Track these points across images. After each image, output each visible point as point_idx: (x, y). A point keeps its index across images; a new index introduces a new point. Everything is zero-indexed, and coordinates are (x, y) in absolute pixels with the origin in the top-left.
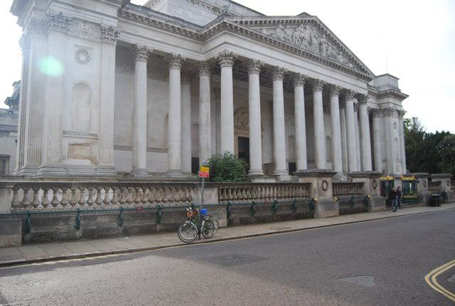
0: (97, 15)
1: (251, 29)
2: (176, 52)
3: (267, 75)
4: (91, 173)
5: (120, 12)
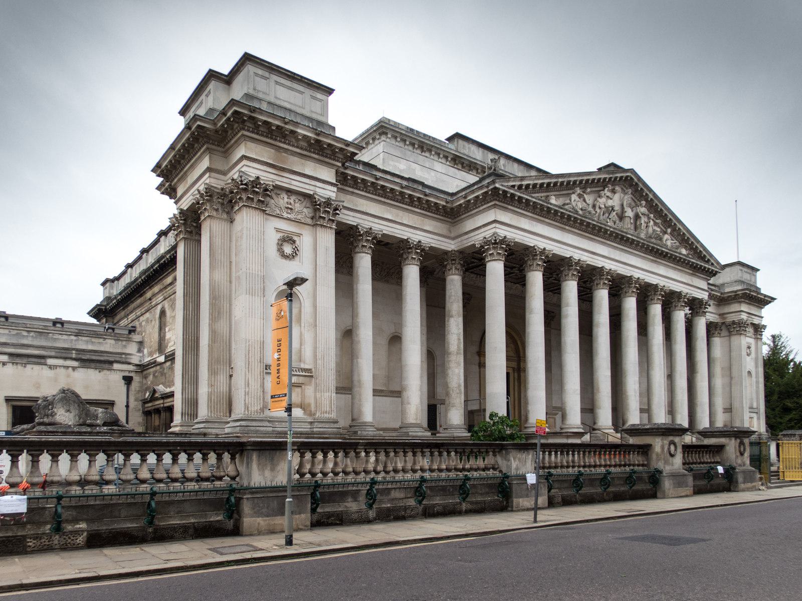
1: (535, 198)
2: (415, 236)
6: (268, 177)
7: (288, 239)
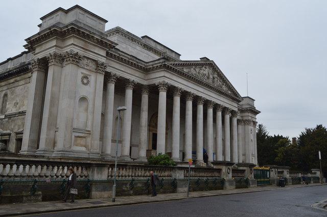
0: (95, 55)
1: (178, 68)
2: (132, 78)
3: (185, 96)
4: (86, 156)
5: (107, 53)
6: (81, 52)
7: (86, 77)
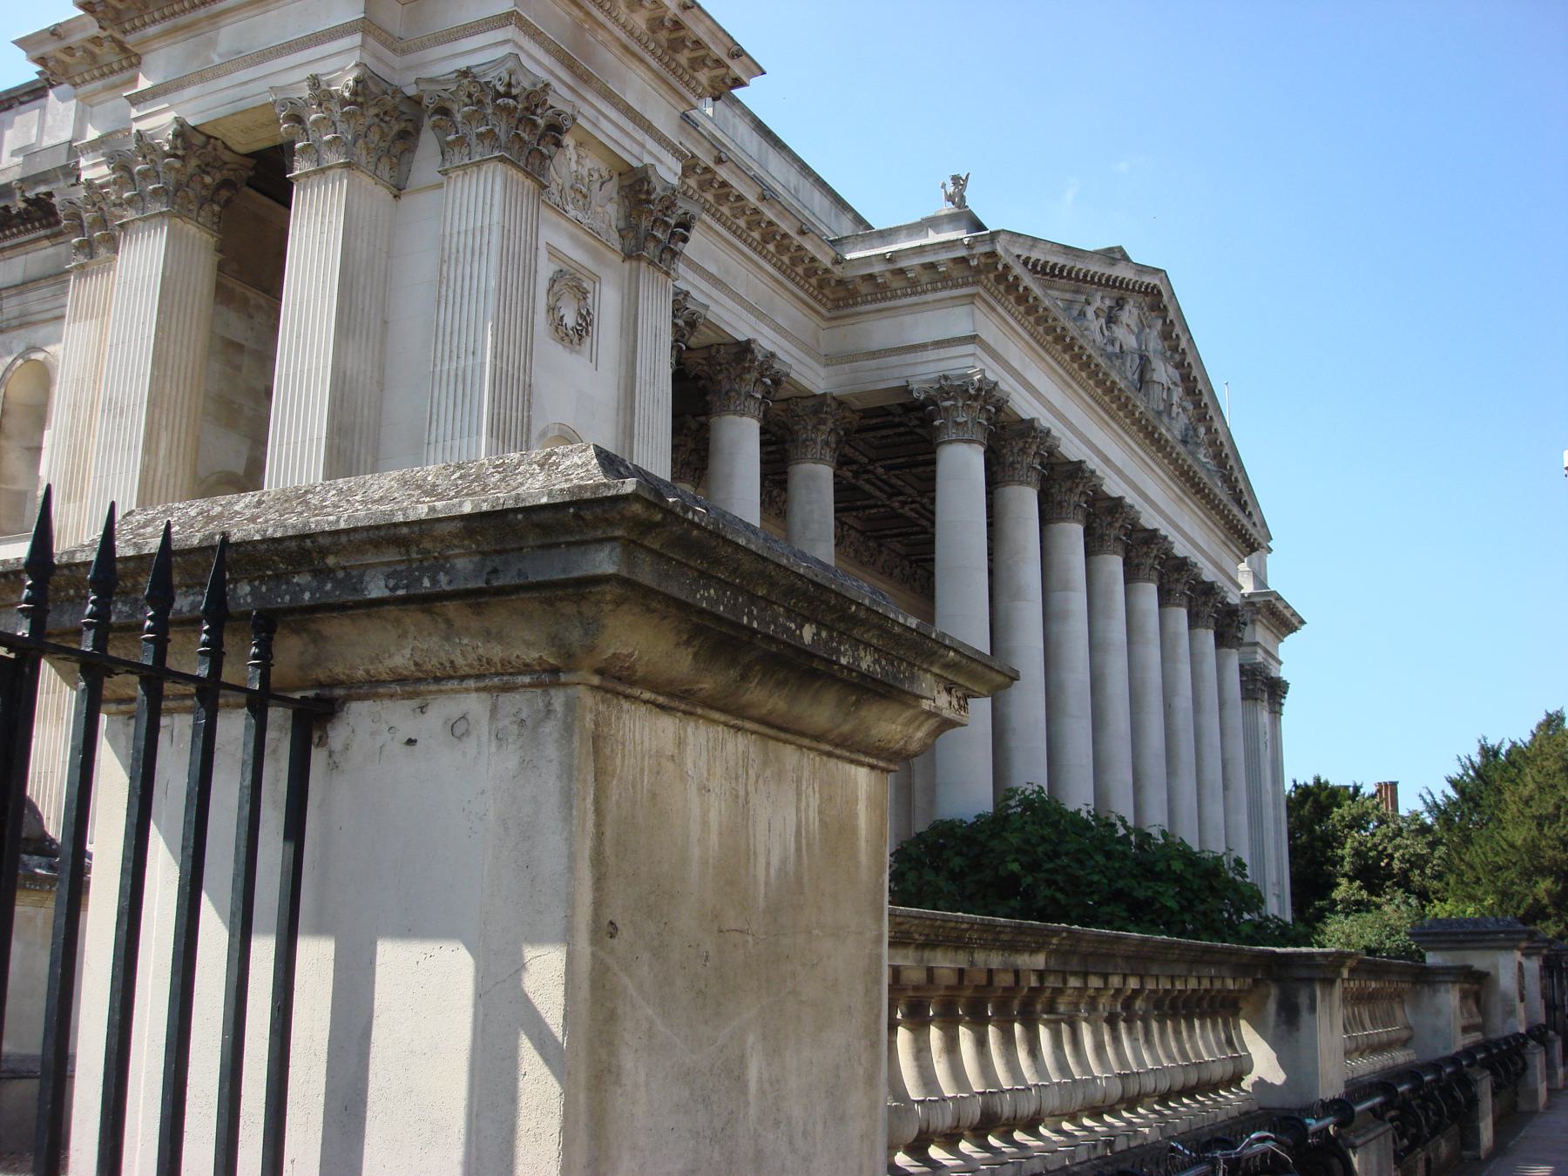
0: (629, 126)
